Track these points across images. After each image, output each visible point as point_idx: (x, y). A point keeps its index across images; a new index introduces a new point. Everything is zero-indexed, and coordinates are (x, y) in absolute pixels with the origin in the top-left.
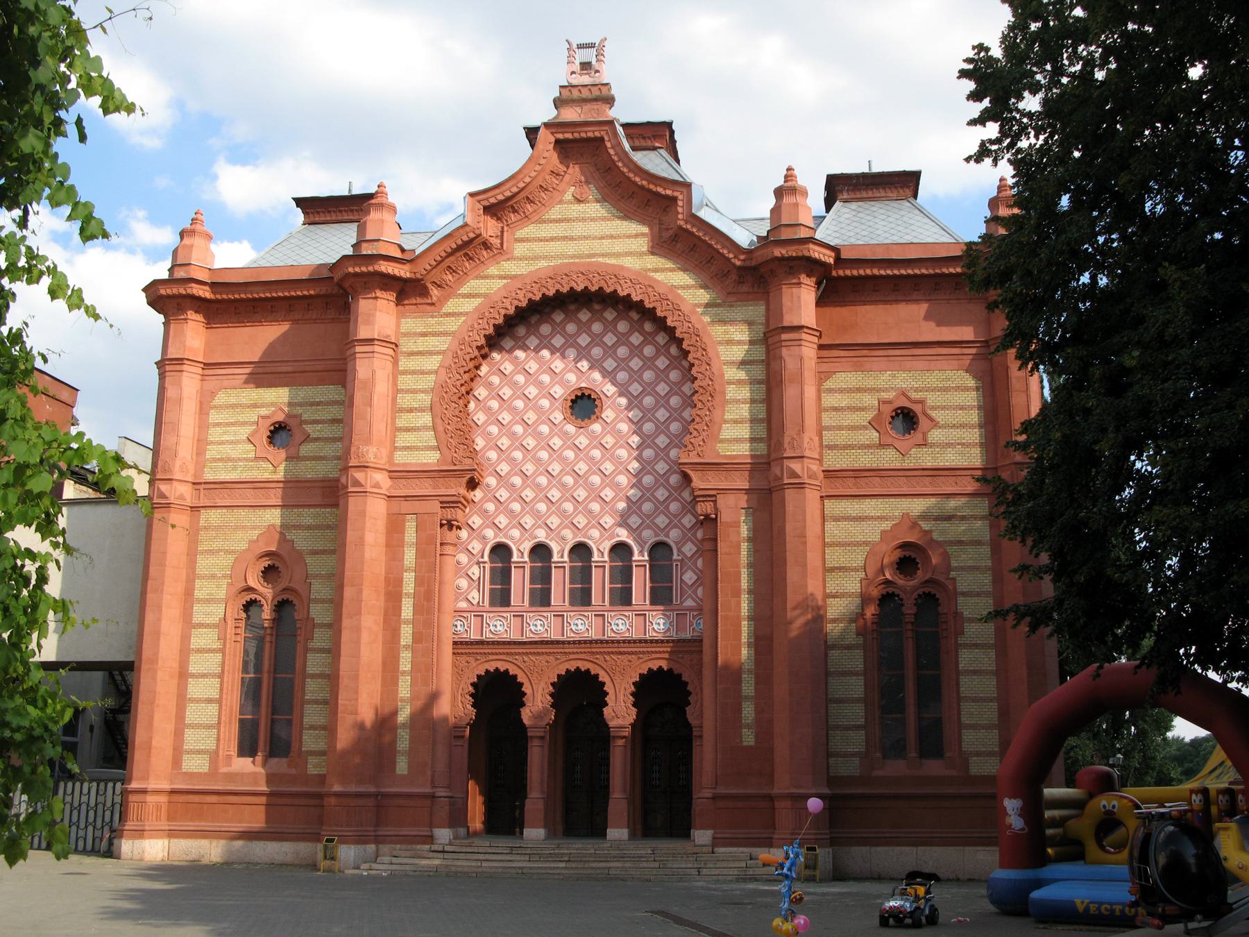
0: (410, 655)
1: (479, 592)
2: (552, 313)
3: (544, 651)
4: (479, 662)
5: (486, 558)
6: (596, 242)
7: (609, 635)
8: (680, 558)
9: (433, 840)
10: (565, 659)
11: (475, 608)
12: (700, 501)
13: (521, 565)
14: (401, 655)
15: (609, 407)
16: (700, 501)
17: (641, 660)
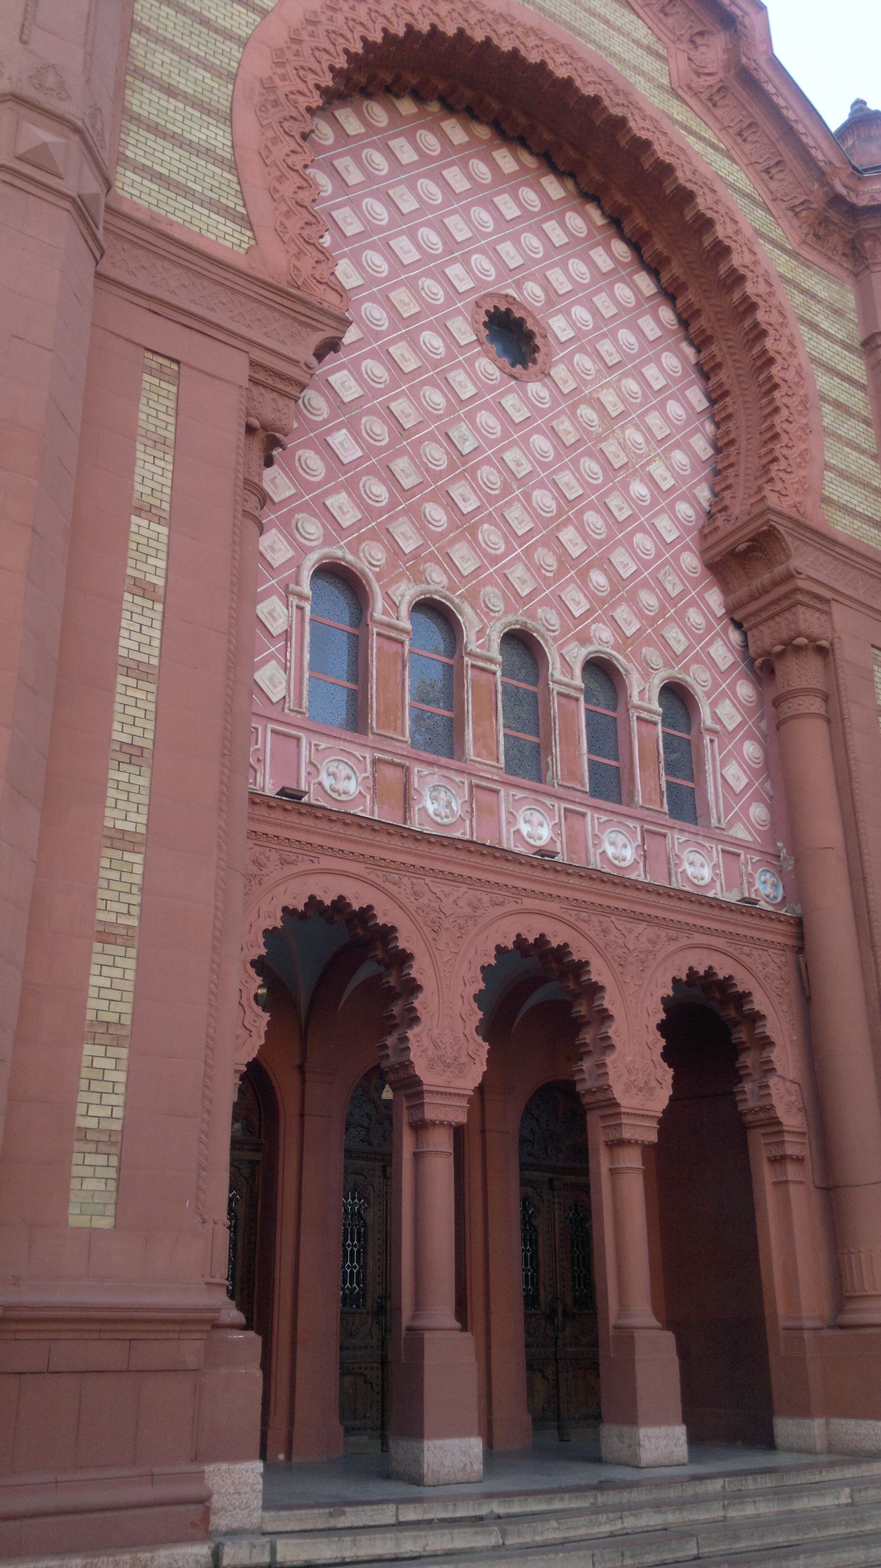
0: (144, 781)
1: (286, 669)
2: (443, 120)
3: (466, 872)
4: (294, 869)
5: (306, 588)
6: (582, 14)
7: (596, 863)
8: (718, 727)
9: (206, 1519)
10: (512, 907)
11: (274, 713)
12: (802, 604)
13: (393, 634)
14: (113, 774)
15: (561, 360)
16: (802, 604)
17: (674, 946)
